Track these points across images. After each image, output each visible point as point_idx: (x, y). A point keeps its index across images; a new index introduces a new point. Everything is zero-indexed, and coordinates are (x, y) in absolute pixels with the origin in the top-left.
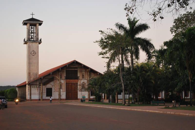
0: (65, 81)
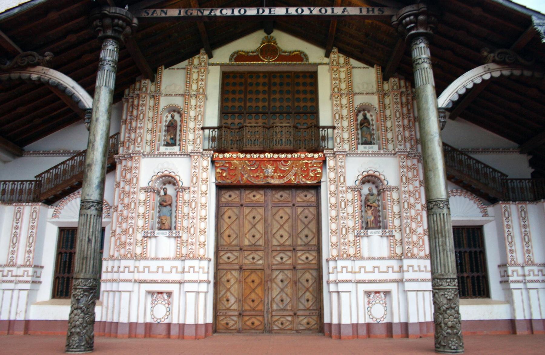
0: (206, 163)
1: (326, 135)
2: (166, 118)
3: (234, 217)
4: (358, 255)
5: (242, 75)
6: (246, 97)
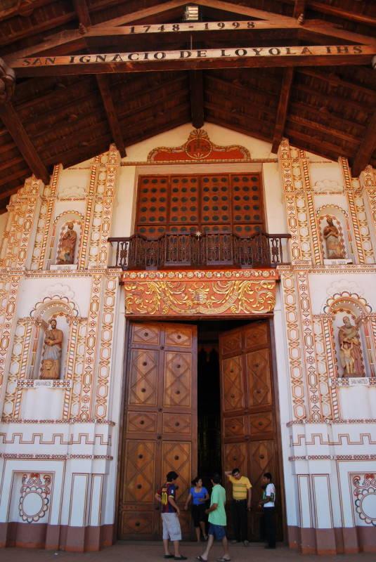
0: (113, 284)
1: (278, 246)
2: (61, 229)
3: (151, 365)
4: (336, 416)
5: (164, 179)
6: (169, 204)
